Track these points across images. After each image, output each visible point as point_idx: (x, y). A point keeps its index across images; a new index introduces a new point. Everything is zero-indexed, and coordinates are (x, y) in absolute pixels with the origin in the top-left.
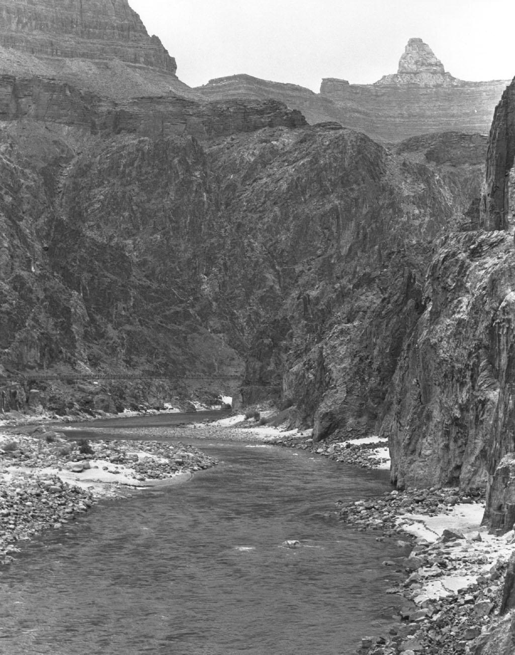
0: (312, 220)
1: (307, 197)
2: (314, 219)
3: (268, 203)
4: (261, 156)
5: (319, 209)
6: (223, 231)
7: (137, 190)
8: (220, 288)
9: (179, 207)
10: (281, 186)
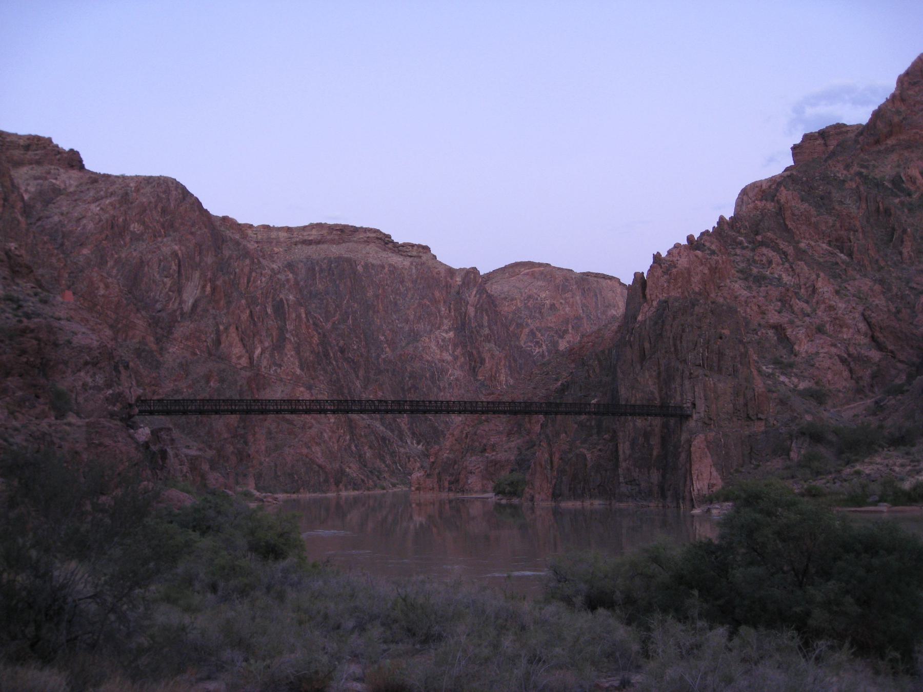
0: (148, 265)
1: (128, 239)
2: (150, 264)
5: (155, 252)
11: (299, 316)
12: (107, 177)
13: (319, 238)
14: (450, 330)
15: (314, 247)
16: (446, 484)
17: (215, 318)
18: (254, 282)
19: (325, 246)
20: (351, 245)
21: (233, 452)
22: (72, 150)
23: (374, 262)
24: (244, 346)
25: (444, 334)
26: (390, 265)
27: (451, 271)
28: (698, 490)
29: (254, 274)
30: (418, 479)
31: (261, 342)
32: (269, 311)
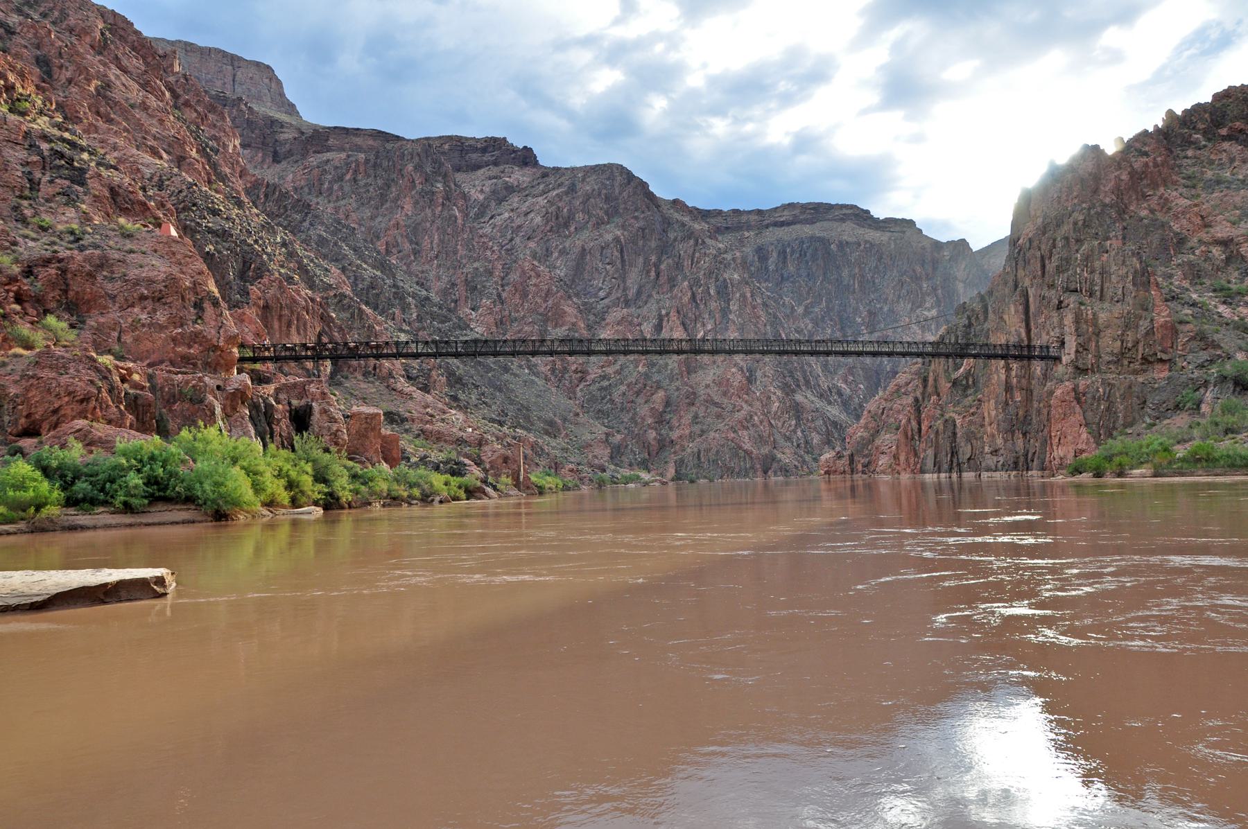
0: (590, 252)
1: (572, 229)
3: (518, 240)
4: (494, 192)
5: (596, 239)
6: (489, 253)
7: (354, 205)
8: (497, 327)
9: (420, 224)
10: (532, 219)
11: (743, 296)
12: (557, 169)
13: (791, 219)
14: (932, 307)
15: (786, 229)
16: (860, 467)
17: (658, 303)
18: (698, 262)
19: (798, 226)
20: (825, 224)
21: (655, 438)
22: (525, 147)
23: (850, 240)
24: (686, 329)
25: (925, 313)
26: (866, 242)
27: (937, 245)
28: (1061, 459)
29: (697, 255)
30: (827, 461)
31: (704, 325)
32: (712, 292)
